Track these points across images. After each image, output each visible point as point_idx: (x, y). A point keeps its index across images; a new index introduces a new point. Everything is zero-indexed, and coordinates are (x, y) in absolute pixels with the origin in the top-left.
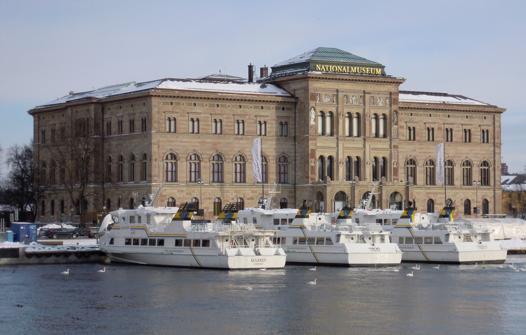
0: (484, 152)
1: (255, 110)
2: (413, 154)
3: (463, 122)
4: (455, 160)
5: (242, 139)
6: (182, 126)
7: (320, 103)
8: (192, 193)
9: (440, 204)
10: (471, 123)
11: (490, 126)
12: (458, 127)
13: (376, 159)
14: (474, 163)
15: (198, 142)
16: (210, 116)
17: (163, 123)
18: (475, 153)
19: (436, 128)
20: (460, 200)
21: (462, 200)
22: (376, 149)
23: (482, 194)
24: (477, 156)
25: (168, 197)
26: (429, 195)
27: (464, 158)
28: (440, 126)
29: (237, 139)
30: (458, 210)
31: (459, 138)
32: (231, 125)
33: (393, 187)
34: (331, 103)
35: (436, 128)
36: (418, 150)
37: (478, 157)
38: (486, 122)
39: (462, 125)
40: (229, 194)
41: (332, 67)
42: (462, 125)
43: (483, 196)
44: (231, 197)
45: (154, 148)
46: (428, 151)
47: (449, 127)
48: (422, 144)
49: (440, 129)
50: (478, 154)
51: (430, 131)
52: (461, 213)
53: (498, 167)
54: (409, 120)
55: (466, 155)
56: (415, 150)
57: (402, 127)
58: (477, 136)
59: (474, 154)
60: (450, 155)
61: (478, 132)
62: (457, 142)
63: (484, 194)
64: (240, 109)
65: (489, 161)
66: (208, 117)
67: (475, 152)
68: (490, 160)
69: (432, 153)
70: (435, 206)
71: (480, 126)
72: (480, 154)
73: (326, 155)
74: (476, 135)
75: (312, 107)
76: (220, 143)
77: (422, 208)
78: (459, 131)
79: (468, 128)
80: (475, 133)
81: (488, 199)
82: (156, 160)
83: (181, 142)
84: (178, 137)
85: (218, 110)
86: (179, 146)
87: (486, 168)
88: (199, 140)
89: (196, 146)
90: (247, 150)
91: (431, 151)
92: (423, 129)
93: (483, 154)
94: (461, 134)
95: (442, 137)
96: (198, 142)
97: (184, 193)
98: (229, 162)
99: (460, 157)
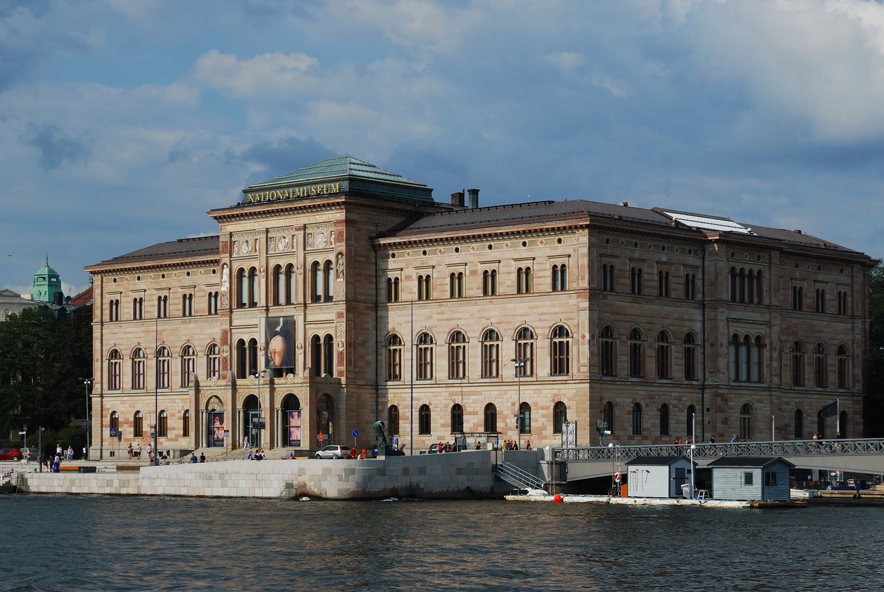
0: (557, 310)
1: (206, 276)
2: (428, 324)
3: (517, 256)
4: (500, 329)
5: (190, 322)
6: (125, 311)
7: (237, 256)
8: (135, 405)
9: (475, 413)
10: (531, 255)
11: (569, 256)
12: (508, 266)
13: (316, 338)
14: (537, 331)
15: (143, 332)
16: (155, 292)
17: (105, 309)
18: (541, 312)
19: (467, 273)
20: (510, 405)
21: (513, 404)
22: (311, 323)
23: (553, 391)
24: (543, 317)
25: (110, 412)
26: (453, 397)
27: (517, 323)
28: (474, 268)
29: (184, 322)
30: (506, 425)
31: (508, 286)
32: (178, 302)
33: (284, 386)
34: (252, 254)
35: (467, 273)
36: (435, 317)
37: (546, 320)
38: (561, 249)
39: (516, 260)
40: (174, 404)
41: (269, 194)
42: (516, 260)
43: (555, 395)
44: (178, 408)
45: (96, 345)
46: (454, 316)
47: (489, 267)
48: (442, 305)
49: (474, 273)
50: (545, 314)
51: (457, 279)
52: (511, 429)
53: (583, 337)
54: (421, 264)
55: (522, 319)
56: (430, 317)
57: (409, 278)
58: (542, 280)
59: (539, 314)
60: (493, 320)
61: (547, 270)
62: (505, 296)
63: (557, 392)
64: (188, 277)
65: (568, 326)
66: (152, 295)
67: (540, 310)
68: (569, 324)
69: (460, 319)
70: (464, 417)
71: (550, 257)
72: (551, 314)
73: (247, 339)
74: (541, 277)
75: (226, 264)
76: (165, 330)
77: (443, 421)
78: (510, 273)
79: (524, 265)
80: (539, 274)
81: (565, 401)
82: (97, 360)
83: (125, 333)
84: (121, 326)
85: (164, 283)
86: (123, 338)
87: (565, 340)
88: (143, 329)
89: (140, 338)
90: (196, 337)
91: (459, 316)
92: (444, 276)
93: (555, 314)
94: (514, 276)
95: (478, 289)
96: (143, 332)
97: (127, 405)
98: (177, 358)
99: (510, 323)
